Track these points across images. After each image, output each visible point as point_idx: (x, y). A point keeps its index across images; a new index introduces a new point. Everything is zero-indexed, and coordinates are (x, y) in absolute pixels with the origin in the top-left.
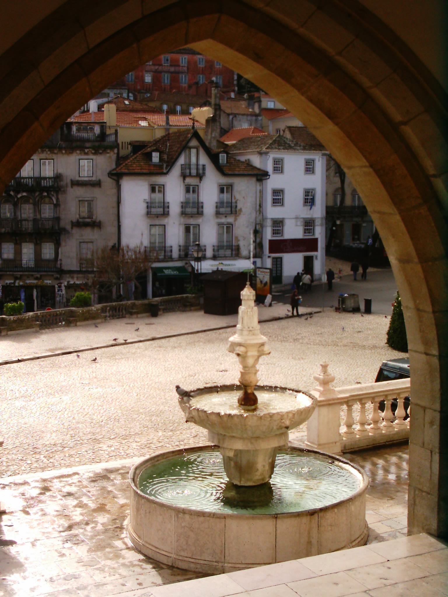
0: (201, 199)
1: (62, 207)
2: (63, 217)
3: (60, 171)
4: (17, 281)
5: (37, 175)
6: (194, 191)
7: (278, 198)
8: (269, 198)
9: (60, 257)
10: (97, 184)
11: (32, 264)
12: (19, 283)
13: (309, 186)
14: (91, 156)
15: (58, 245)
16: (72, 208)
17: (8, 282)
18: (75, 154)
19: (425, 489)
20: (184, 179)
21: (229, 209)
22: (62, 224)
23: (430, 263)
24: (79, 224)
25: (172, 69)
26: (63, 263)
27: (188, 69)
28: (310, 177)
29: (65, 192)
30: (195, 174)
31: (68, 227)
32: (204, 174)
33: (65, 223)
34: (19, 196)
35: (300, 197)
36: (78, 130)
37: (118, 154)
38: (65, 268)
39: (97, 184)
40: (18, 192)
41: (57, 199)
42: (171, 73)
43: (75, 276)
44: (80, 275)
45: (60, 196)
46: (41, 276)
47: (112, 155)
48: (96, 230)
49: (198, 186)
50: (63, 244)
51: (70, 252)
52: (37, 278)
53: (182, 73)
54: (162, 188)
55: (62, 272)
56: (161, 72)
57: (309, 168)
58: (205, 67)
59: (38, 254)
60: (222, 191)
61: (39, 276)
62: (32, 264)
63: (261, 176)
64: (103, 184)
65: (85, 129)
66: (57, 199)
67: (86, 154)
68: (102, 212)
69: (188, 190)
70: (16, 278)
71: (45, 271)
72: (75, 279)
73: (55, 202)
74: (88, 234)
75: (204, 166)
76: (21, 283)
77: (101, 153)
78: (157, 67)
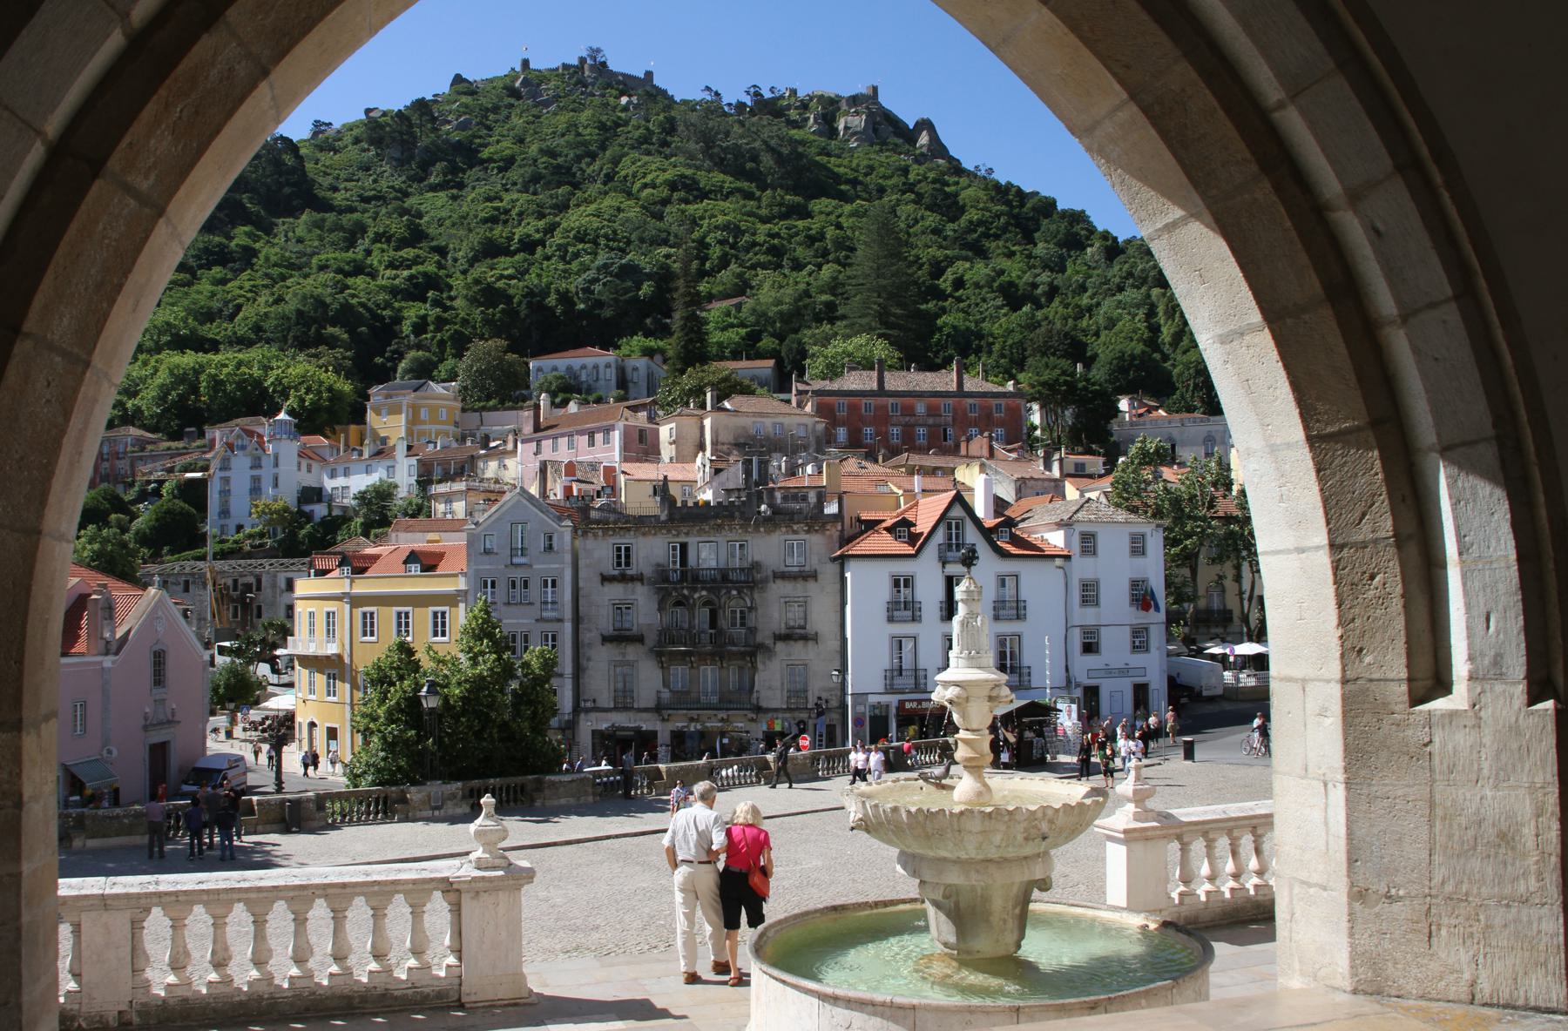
1: (760, 611)
2: (760, 627)
14: (803, 536)
15: (754, 668)
16: (774, 609)
19: (1315, 878)
20: (944, 564)
22: (759, 639)
23: (1289, 321)
24: (787, 637)
25: (931, 421)
27: (954, 419)
28: (1139, 560)
29: (763, 590)
31: (769, 642)
33: (763, 637)
34: (696, 596)
36: (785, 498)
37: (842, 531)
38: (764, 704)
39: (813, 576)
40: (695, 590)
41: (752, 600)
45: (756, 596)
48: (810, 643)
50: (760, 666)
52: (722, 720)
54: (909, 582)
55: (758, 709)
56: (913, 426)
62: (715, 699)
65: (795, 498)
66: (752, 600)
67: (795, 532)
68: (820, 618)
70: (692, 720)
74: (798, 651)
76: (699, 727)
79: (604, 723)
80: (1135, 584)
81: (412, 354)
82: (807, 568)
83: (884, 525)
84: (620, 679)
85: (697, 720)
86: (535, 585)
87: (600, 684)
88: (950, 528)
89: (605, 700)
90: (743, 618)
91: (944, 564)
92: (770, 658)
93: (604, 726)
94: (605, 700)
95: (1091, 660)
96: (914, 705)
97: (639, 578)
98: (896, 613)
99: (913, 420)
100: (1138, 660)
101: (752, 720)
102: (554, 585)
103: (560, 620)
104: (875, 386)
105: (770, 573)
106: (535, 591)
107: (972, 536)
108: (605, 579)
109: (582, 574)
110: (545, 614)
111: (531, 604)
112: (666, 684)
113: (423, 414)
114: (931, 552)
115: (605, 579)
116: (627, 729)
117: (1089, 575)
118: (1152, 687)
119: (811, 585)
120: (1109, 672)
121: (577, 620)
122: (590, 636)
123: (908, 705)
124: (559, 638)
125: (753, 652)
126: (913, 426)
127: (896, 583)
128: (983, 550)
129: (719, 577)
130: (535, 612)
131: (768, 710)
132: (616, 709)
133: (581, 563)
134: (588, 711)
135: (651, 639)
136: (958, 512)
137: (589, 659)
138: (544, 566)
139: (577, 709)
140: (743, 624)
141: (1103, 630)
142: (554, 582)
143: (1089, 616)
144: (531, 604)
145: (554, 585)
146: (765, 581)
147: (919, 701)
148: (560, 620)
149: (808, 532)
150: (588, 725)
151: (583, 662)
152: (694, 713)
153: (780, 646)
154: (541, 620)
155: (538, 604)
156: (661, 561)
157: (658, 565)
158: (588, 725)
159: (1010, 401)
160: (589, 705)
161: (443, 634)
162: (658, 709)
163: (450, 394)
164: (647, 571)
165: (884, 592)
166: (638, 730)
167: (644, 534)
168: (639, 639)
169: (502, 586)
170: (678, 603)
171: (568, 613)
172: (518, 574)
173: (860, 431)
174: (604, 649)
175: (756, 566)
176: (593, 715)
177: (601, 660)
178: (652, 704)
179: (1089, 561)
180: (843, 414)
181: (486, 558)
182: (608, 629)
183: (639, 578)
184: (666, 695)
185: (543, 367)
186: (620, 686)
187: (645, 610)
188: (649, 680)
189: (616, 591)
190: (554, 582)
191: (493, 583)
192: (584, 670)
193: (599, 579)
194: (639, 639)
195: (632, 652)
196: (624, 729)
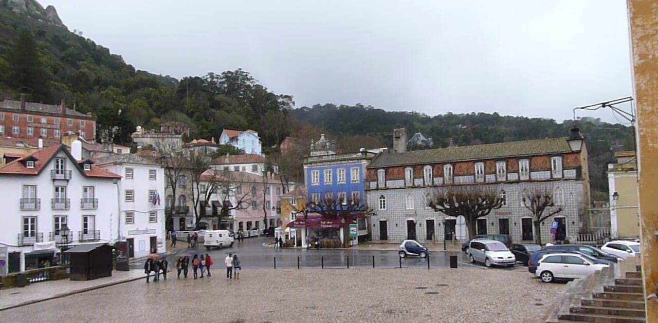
0: (68, 197)
7: (130, 195)
25: (49, 126)
27: (60, 127)
32: (70, 177)
35: (146, 196)
42: (48, 128)
49: (65, 186)
53: (57, 129)
56: (40, 128)
57: (153, 176)
58: (73, 126)
60: (85, 190)
63: (116, 179)
69: (57, 190)
75: (71, 171)
78: (37, 124)
80: (151, 192)
88: (58, 162)
91: (54, 180)
95: (130, 227)
99: (39, 125)
100: (152, 226)
104: (20, 108)
117: (129, 188)
118: (158, 238)
120: (138, 232)
126: (40, 128)
141: (136, 213)
143: (129, 206)
173: (11, 128)
179: (130, 181)
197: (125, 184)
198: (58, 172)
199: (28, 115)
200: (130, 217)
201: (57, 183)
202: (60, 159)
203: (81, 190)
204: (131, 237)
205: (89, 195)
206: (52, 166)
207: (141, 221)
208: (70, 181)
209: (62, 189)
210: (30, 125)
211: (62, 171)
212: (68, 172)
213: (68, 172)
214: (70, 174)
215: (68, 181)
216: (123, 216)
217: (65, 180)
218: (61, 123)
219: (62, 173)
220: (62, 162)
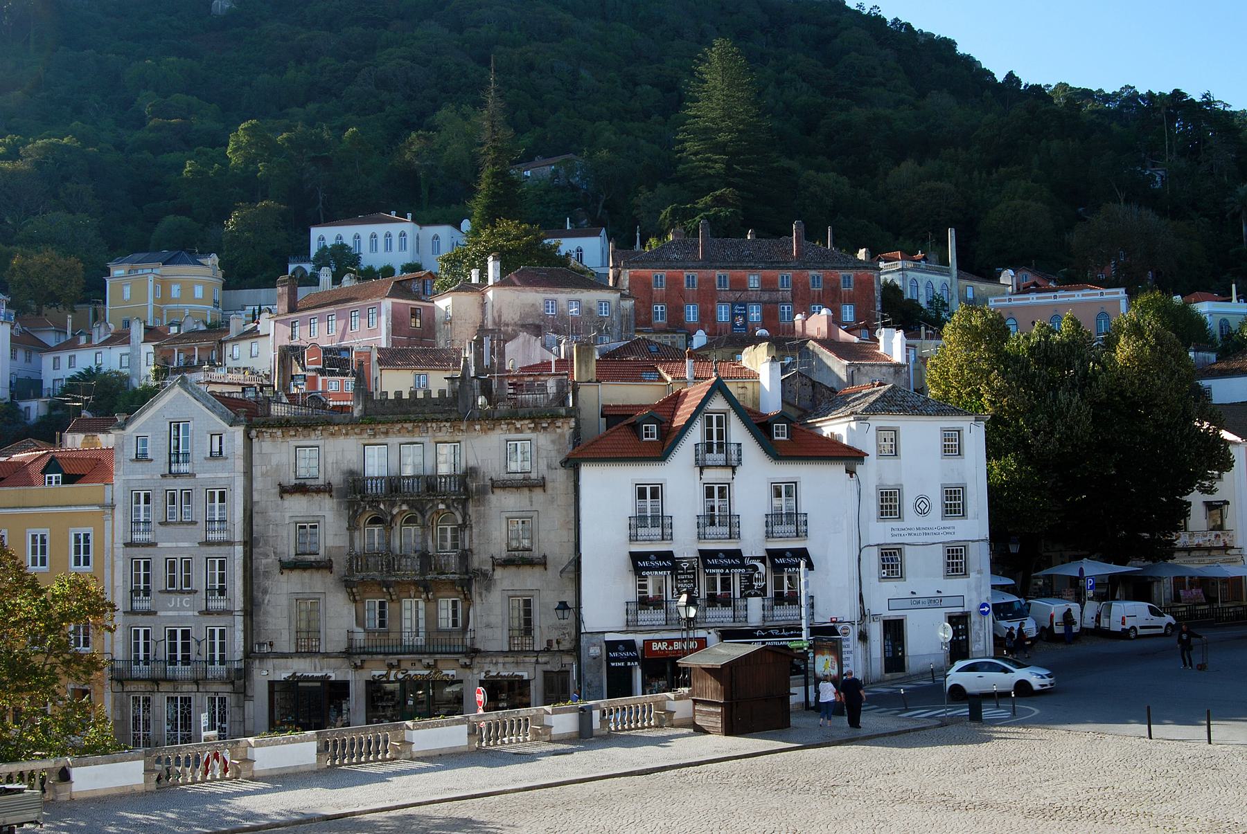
3: (472, 463)
4: (393, 672)
5: (429, 472)
6: (722, 495)
8: (872, 504)
9: (471, 626)
10: (541, 484)
11: (421, 640)
12: (395, 676)
13: (954, 480)
15: (468, 599)
17: (377, 673)
18: (498, 432)
20: (701, 473)
21: (793, 528)
22: (475, 563)
24: (507, 563)
25: (766, 297)
26: (479, 635)
28: (954, 462)
30: (722, 463)
31: (488, 567)
32: (739, 461)
34: (395, 511)
39: (541, 484)
40: (393, 505)
41: (465, 515)
42: (765, 303)
43: (501, 660)
44: (510, 659)
45: (471, 510)
46: (436, 661)
47: (566, 428)
51: (491, 619)
52: (428, 667)
53: (784, 302)
55: (473, 652)
57: (952, 446)
59: (432, 618)
61: (432, 662)
62: (421, 640)
64: (549, 485)
65: (530, 388)
67: (518, 430)
69: (709, 493)
70: (391, 667)
71: (442, 653)
72: (500, 666)
73: (460, 522)
75: (739, 445)
76: (400, 676)
77: (545, 428)
79: (283, 672)
81: (170, 219)
82: (534, 476)
83: (630, 420)
84: (304, 615)
85: (398, 667)
86: (199, 498)
87: (279, 624)
88: (709, 420)
89: (285, 643)
90: (454, 538)
92: (488, 589)
93: (284, 675)
94: (285, 643)
95: (893, 588)
96: (664, 646)
97: (327, 489)
98: (641, 531)
100: (956, 586)
101: (465, 666)
102: (222, 499)
103: (230, 543)
105: (489, 483)
106: (198, 509)
107: (737, 432)
108: (285, 491)
109: (257, 485)
110: (211, 536)
111: (194, 523)
112: (360, 621)
113: (175, 291)
114: (685, 452)
115: (285, 491)
116: (313, 679)
117: (890, 482)
119: (538, 494)
120: (916, 602)
121: (250, 543)
122: (265, 562)
123: (655, 647)
124: (228, 565)
125: (468, 580)
126: (743, 304)
127: (641, 494)
128: (752, 451)
129: (422, 487)
130: (199, 533)
131: (487, 654)
132: (298, 654)
133: (257, 471)
134: (264, 657)
135: (340, 566)
136: (718, 404)
137: (265, 592)
138: (209, 475)
139: (249, 654)
140: (455, 546)
141: (907, 549)
142: (222, 495)
144: (194, 523)
145: (222, 499)
146: (482, 492)
147: (670, 642)
148: (230, 543)
149: (534, 430)
150: (266, 673)
151: (258, 594)
152: (393, 660)
153: (499, 573)
154: (208, 543)
155: (202, 524)
156: (356, 467)
157: (351, 473)
158: (266, 673)
159: (860, 273)
160: (265, 649)
161: (87, 563)
162: (349, 653)
163: (209, 271)
164: (336, 479)
165: (627, 504)
166: (324, 680)
167: (332, 434)
168: (325, 566)
169: (158, 500)
170: (375, 521)
171: (238, 536)
172: (178, 485)
174: (284, 578)
175: (471, 472)
176: (270, 663)
177: (282, 592)
178: (342, 646)
180: (659, 289)
181: (138, 465)
182: (290, 554)
183: (327, 489)
184: (360, 637)
185: (323, 236)
186: (303, 625)
187: (332, 531)
188: (340, 618)
189: (298, 506)
190: (222, 495)
191: (147, 501)
192: (259, 605)
193: (277, 490)
194: (325, 566)
195: (316, 582)
196: (308, 679)
197: (873, 472)
198: (710, 450)
199: (718, 272)
200: (891, 561)
201: (712, 475)
202: (714, 416)
203: (765, 492)
204: (893, 615)
205: (782, 503)
206: (696, 435)
207: (924, 572)
208: (738, 470)
209: (721, 490)
210: (723, 296)
211: (720, 446)
212: (734, 448)
213: (734, 448)
214: (739, 452)
215: (734, 468)
216: (872, 559)
217: (726, 466)
218: (794, 284)
219: (720, 450)
220: (719, 424)
